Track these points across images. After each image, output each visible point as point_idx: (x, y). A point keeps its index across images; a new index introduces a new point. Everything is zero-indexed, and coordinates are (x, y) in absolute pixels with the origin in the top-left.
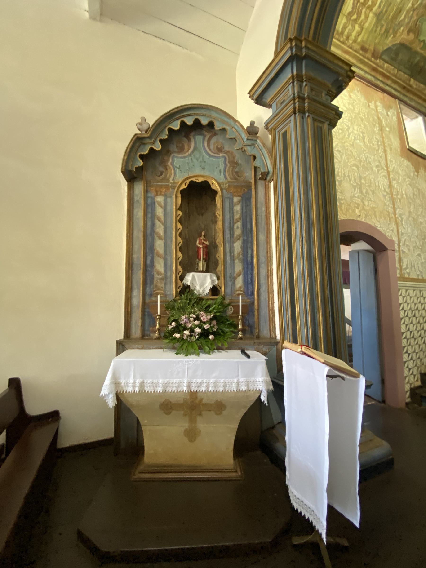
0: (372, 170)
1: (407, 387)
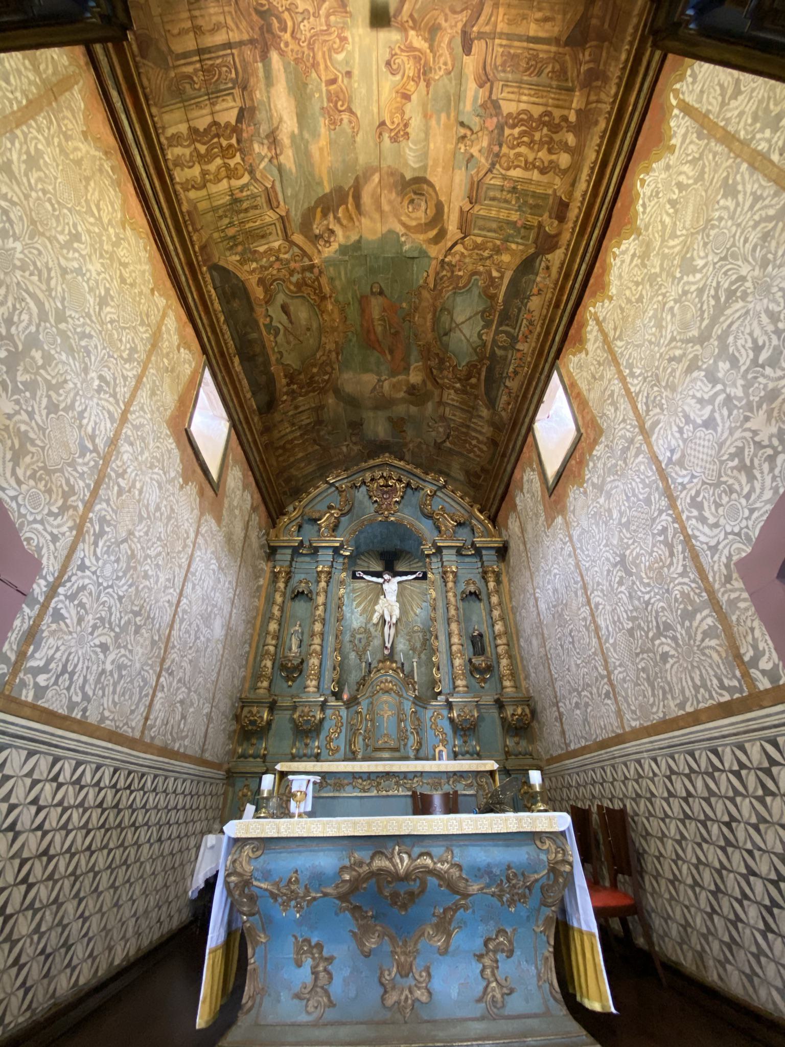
0: (86, 370)
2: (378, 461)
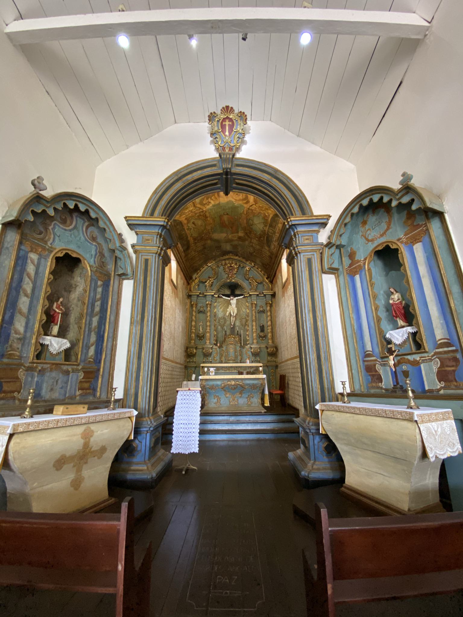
2: (227, 257)
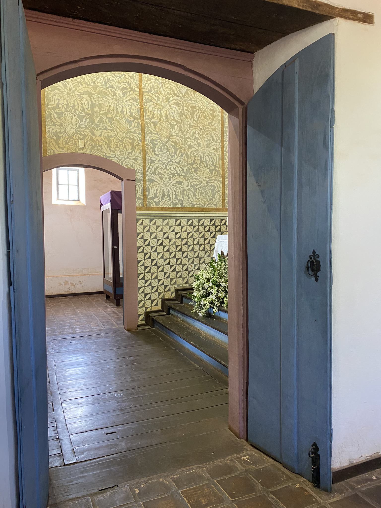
0: (115, 94)
1: (141, 311)
